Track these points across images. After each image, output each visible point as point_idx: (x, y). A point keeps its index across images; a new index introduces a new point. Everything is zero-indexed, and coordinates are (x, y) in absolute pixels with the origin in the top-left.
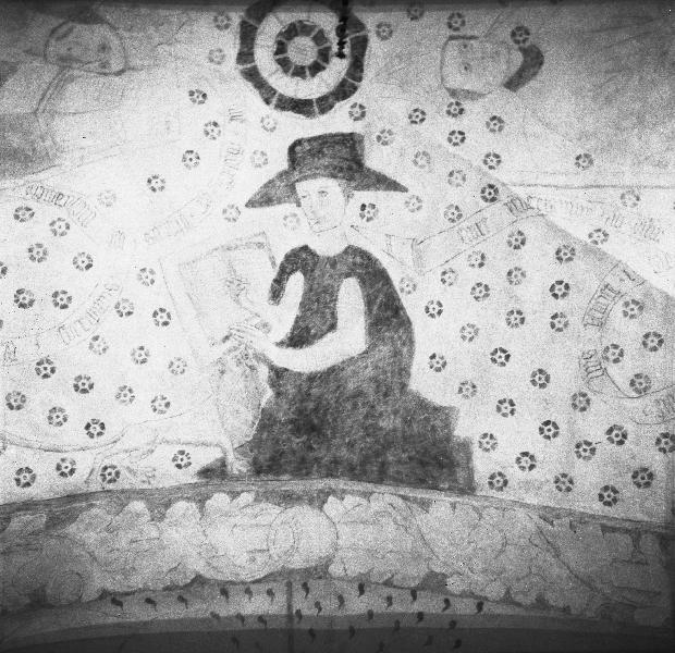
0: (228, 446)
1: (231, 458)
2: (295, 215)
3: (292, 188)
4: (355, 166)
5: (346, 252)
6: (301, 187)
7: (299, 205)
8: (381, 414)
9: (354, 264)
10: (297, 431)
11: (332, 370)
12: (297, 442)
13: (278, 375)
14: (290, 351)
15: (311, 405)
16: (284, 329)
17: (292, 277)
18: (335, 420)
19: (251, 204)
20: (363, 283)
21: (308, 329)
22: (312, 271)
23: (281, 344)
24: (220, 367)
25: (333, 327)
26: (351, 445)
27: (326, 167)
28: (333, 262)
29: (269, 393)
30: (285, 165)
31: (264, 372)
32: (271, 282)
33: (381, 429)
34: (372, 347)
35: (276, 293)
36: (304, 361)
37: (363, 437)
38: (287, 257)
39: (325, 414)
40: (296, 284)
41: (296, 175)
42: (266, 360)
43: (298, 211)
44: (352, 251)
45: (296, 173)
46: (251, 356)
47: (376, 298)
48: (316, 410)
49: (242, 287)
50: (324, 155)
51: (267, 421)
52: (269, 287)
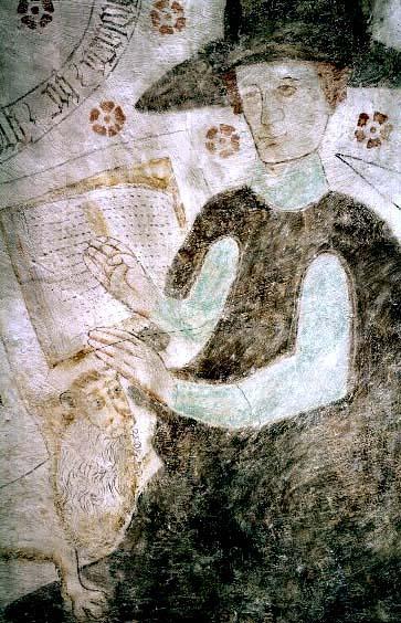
0: (71, 566)
1: (72, 586)
2: (229, 129)
3: (228, 75)
4: (350, 38)
5: (323, 203)
6: (246, 74)
7: (238, 110)
8: (370, 526)
9: (338, 228)
10: (203, 541)
11: (280, 430)
12: (202, 563)
13: (176, 430)
14: (204, 388)
15: (236, 494)
16: (184, 353)
17: (215, 247)
18: (278, 526)
19: (148, 103)
20: (350, 257)
21: (239, 348)
22: (256, 236)
23: (185, 372)
24: (65, 408)
25: (286, 347)
26: (306, 579)
27: (298, 38)
28: (297, 222)
29: (155, 464)
30: (217, 32)
31: (145, 425)
32: (175, 252)
33: (368, 554)
34: (361, 391)
35: (182, 276)
36: (238, 406)
37: (333, 568)
38: (211, 208)
39: (261, 514)
40: (226, 253)
41: (239, 52)
42: (155, 404)
43: (239, 125)
44: (335, 202)
45: (239, 48)
46: (125, 390)
47: (375, 294)
48: (244, 502)
49: (116, 260)
50: (295, 17)
51: (151, 516)
52: (170, 263)
